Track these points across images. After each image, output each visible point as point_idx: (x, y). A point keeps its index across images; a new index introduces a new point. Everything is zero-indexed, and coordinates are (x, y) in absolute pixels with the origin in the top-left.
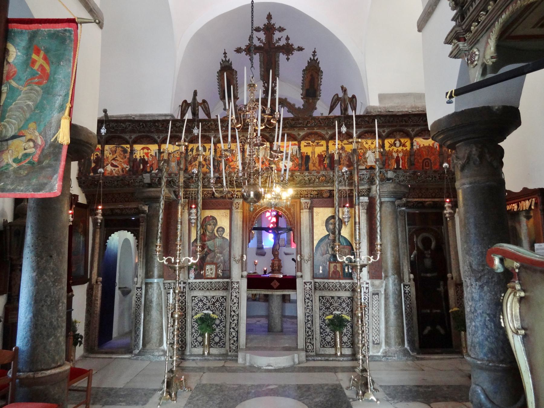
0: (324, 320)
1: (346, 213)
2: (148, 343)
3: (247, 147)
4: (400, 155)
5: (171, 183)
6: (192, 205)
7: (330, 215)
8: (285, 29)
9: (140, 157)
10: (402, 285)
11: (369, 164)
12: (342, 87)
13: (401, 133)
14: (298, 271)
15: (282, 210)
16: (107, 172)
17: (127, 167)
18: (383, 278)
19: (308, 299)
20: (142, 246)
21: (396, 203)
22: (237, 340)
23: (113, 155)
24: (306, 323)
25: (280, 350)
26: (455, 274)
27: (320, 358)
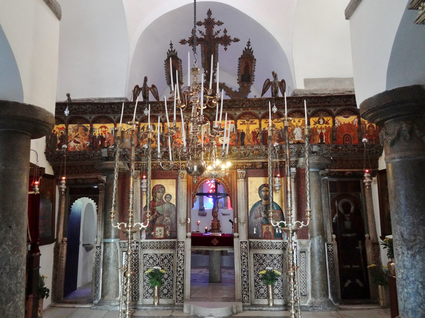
0: (258, 275)
1: (277, 182)
2: (106, 295)
3: (191, 125)
4: (324, 131)
5: (125, 157)
6: (143, 175)
7: (263, 183)
8: (223, 23)
9: (99, 134)
10: (326, 244)
11: (296, 139)
12: (273, 73)
13: (325, 112)
14: (235, 232)
15: (221, 179)
16: (71, 148)
17: (88, 143)
18: (309, 238)
19: (244, 256)
20: (101, 211)
21: (320, 173)
22: (183, 292)
23: (75, 133)
24: (242, 277)
25: (219, 301)
26: (372, 235)
27: (254, 308)
